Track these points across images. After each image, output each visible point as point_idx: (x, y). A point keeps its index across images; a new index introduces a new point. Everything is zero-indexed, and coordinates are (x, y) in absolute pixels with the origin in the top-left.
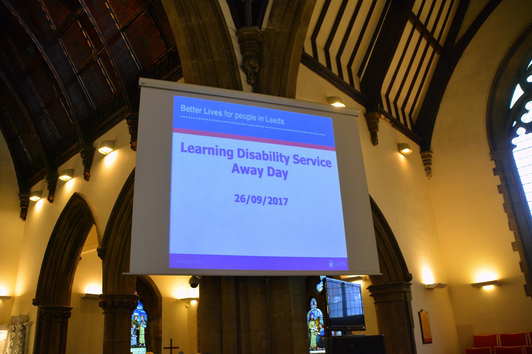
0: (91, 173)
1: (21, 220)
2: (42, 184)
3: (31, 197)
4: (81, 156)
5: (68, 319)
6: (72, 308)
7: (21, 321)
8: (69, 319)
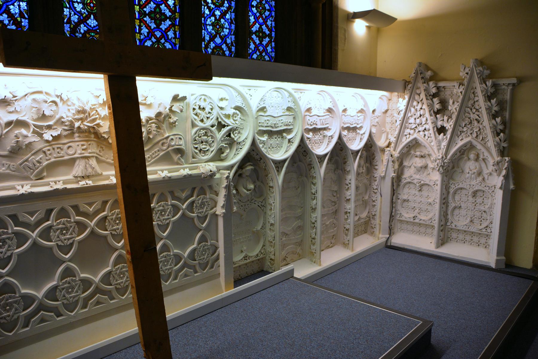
7: (483, 72)
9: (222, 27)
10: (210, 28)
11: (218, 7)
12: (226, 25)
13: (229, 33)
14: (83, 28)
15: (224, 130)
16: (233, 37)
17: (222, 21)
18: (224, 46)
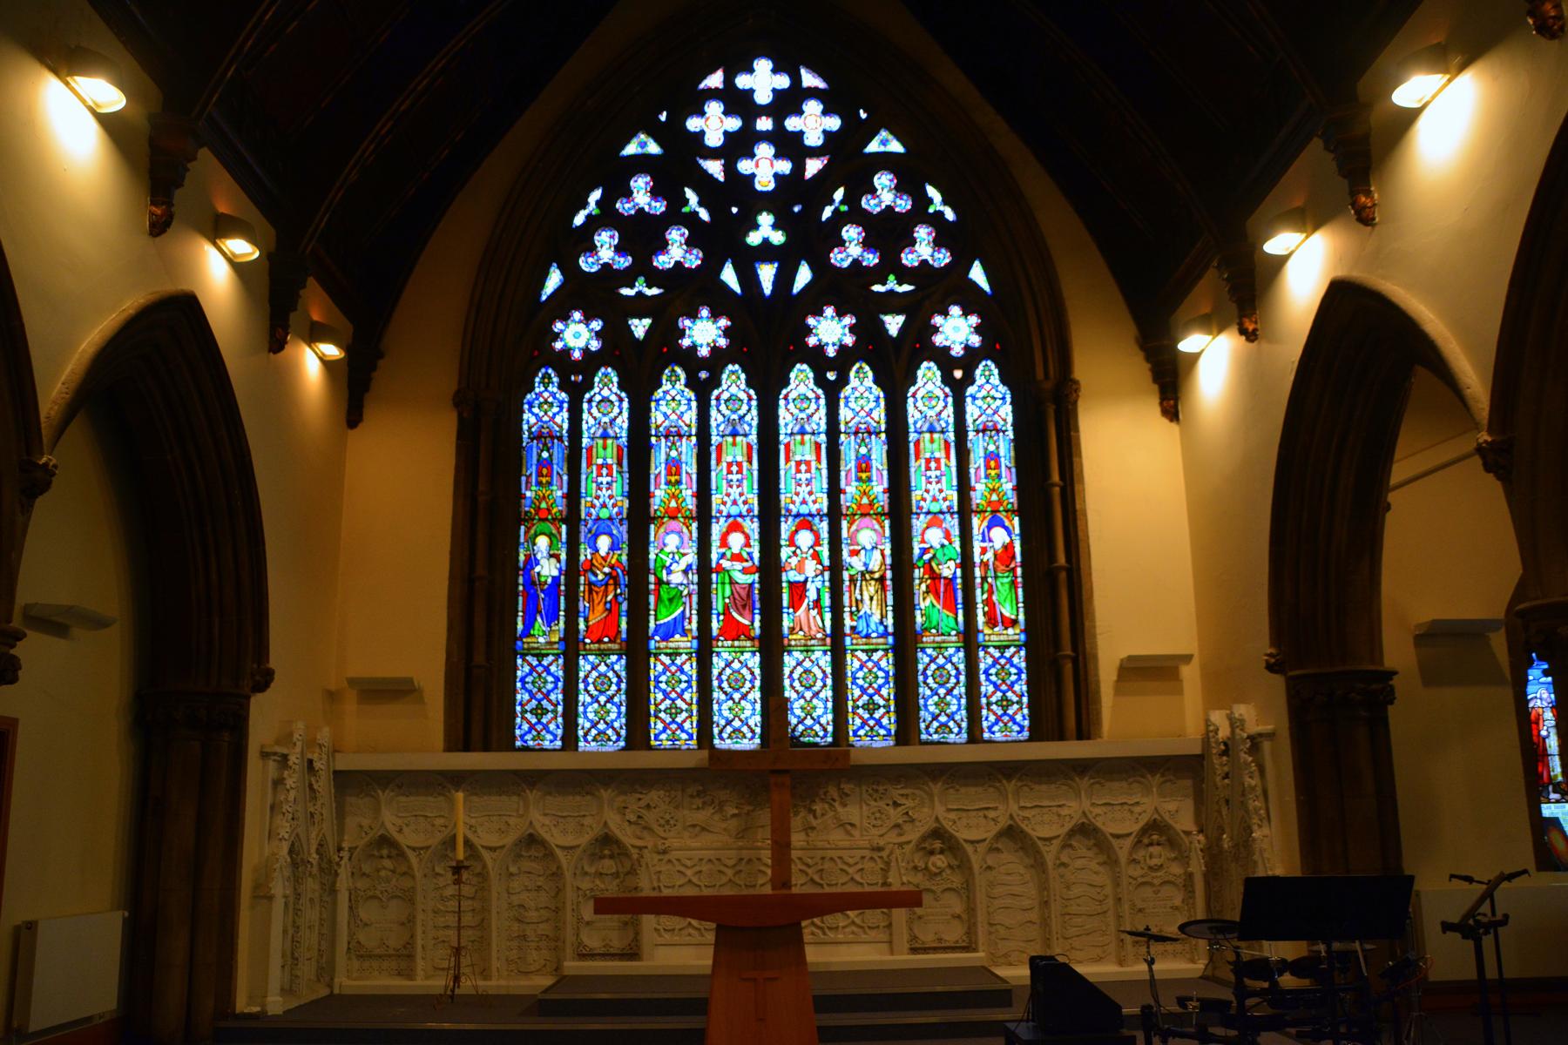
0: (1376, 196)
1: (1165, 421)
2: (1209, 288)
3: (1182, 340)
4: (1327, 148)
5: (1386, 710)
6: (1395, 673)
8: (1390, 707)
9: (948, 704)
10: (932, 709)
11: (941, 685)
12: (955, 701)
13: (959, 709)
14: (801, 728)
15: (900, 809)
16: (964, 712)
17: (948, 698)
18: (951, 724)
